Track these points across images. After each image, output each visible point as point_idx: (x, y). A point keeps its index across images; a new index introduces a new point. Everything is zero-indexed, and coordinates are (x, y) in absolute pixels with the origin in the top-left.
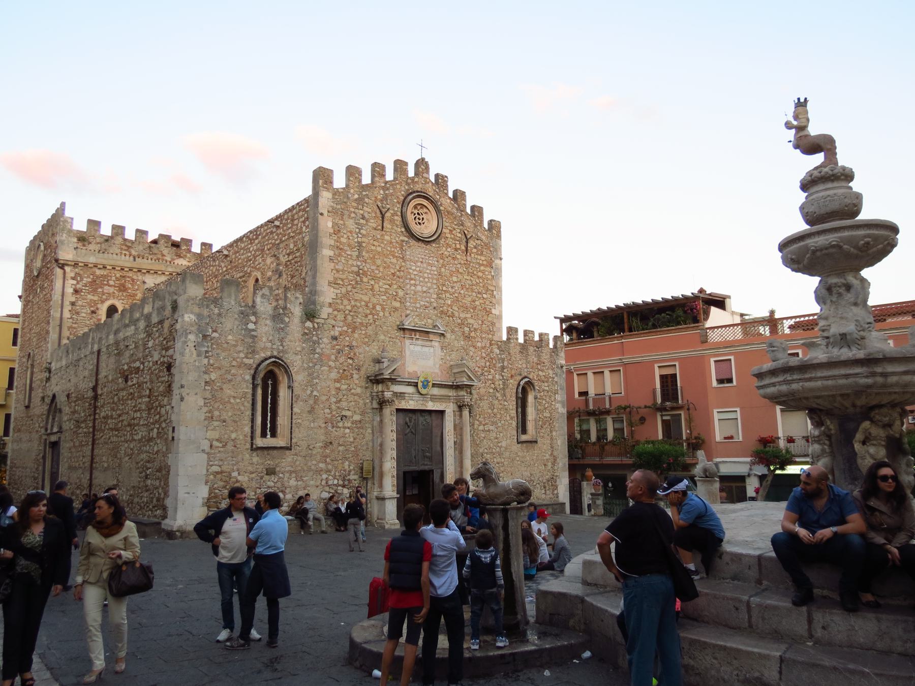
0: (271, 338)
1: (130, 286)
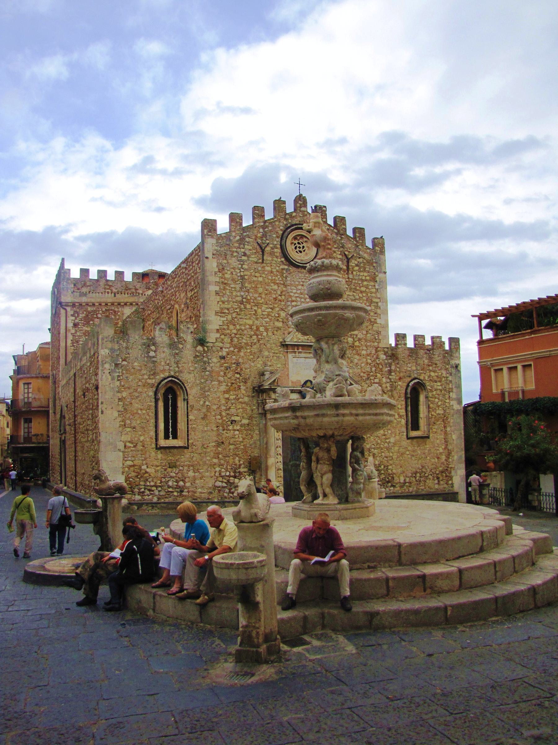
0: (168, 362)
1: (113, 317)
